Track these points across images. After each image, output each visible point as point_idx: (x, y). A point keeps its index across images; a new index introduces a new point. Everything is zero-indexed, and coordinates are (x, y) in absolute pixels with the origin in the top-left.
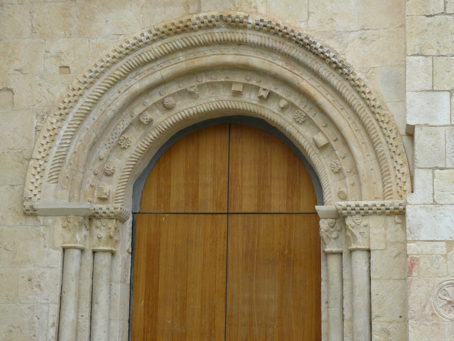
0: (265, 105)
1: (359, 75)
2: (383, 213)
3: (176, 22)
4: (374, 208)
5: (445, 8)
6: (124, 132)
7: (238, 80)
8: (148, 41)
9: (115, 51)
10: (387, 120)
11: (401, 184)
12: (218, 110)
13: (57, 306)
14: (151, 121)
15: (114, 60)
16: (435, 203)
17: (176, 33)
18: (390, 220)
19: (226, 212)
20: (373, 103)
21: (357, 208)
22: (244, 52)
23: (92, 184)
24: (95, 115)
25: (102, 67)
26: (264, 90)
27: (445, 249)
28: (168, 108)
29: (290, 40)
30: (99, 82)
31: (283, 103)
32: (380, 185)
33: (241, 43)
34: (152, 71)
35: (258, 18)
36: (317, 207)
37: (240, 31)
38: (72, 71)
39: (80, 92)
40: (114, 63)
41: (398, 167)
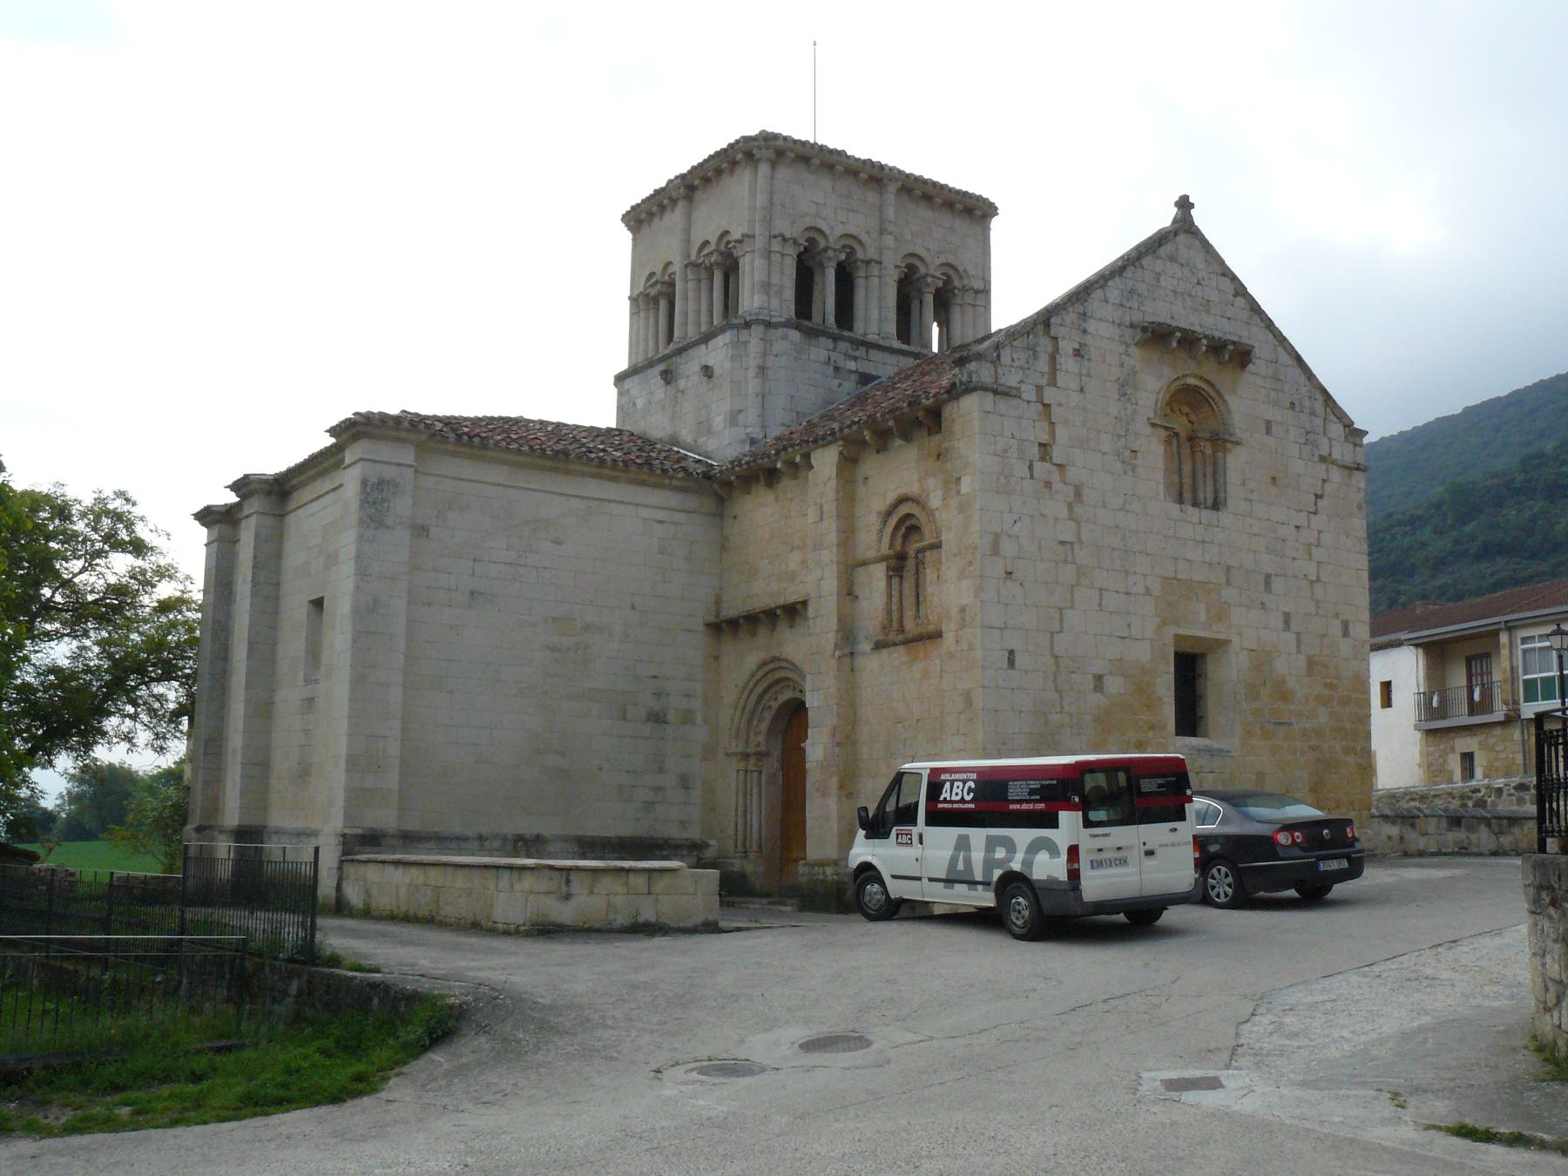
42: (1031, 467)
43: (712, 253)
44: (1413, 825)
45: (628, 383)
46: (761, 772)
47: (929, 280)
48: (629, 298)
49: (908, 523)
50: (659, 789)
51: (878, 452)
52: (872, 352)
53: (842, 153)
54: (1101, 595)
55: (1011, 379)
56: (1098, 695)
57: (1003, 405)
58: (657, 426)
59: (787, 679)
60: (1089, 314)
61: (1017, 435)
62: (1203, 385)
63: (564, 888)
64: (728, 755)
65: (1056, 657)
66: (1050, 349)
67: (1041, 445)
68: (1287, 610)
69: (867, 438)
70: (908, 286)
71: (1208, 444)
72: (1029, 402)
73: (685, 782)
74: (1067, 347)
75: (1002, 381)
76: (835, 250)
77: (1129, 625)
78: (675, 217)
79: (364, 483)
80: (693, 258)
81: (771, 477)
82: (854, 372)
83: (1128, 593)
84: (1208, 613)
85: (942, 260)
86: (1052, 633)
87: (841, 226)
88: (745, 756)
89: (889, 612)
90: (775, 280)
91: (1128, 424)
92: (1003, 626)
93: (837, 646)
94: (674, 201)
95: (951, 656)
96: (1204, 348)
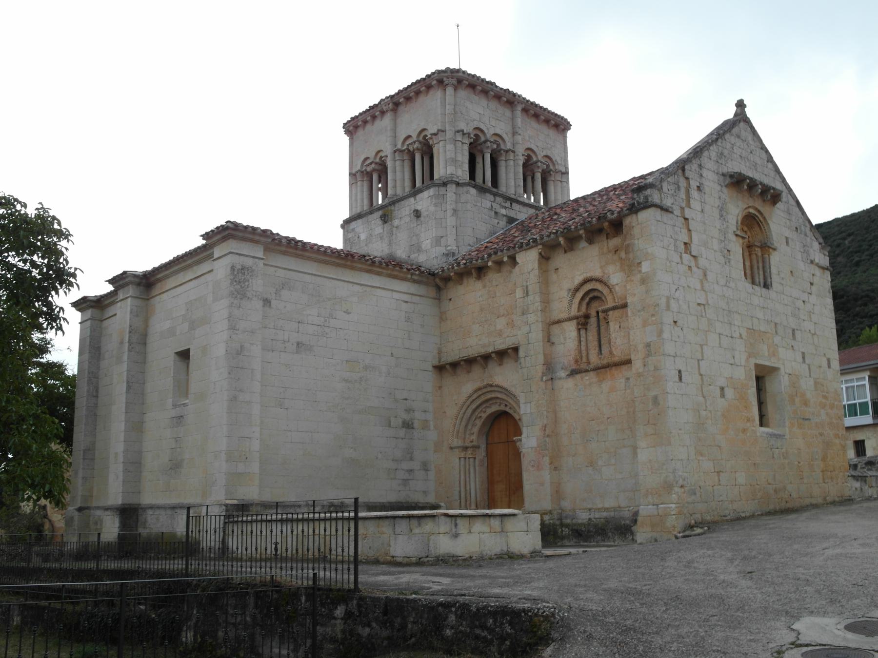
14: (481, 417)
24: (465, 417)
42: (681, 257)
43: (415, 142)
44: (865, 481)
45: (353, 225)
46: (475, 458)
47: (539, 164)
48: (350, 174)
49: (591, 295)
50: (411, 471)
51: (565, 252)
52: (514, 204)
53: (493, 84)
54: (720, 338)
55: (668, 202)
56: (723, 399)
57: (666, 217)
58: (378, 249)
59: (497, 398)
60: (703, 165)
61: (673, 236)
62: (757, 214)
63: (454, 530)
64: (451, 448)
65: (701, 375)
66: (685, 185)
67: (685, 244)
68: (803, 350)
69: (562, 242)
70: (528, 166)
71: (759, 249)
72: (677, 216)
73: (425, 467)
74: (694, 184)
75: (664, 202)
76: (491, 142)
77: (734, 357)
78: (387, 121)
79: (233, 268)
80: (399, 146)
81: (481, 271)
82: (505, 216)
83: (732, 337)
84: (768, 352)
85: (545, 153)
86: (698, 360)
87: (493, 128)
88: (465, 448)
89: (580, 352)
90: (459, 158)
91: (725, 234)
92: (675, 355)
93: (544, 374)
94: (383, 113)
95: (639, 375)
96: (760, 190)
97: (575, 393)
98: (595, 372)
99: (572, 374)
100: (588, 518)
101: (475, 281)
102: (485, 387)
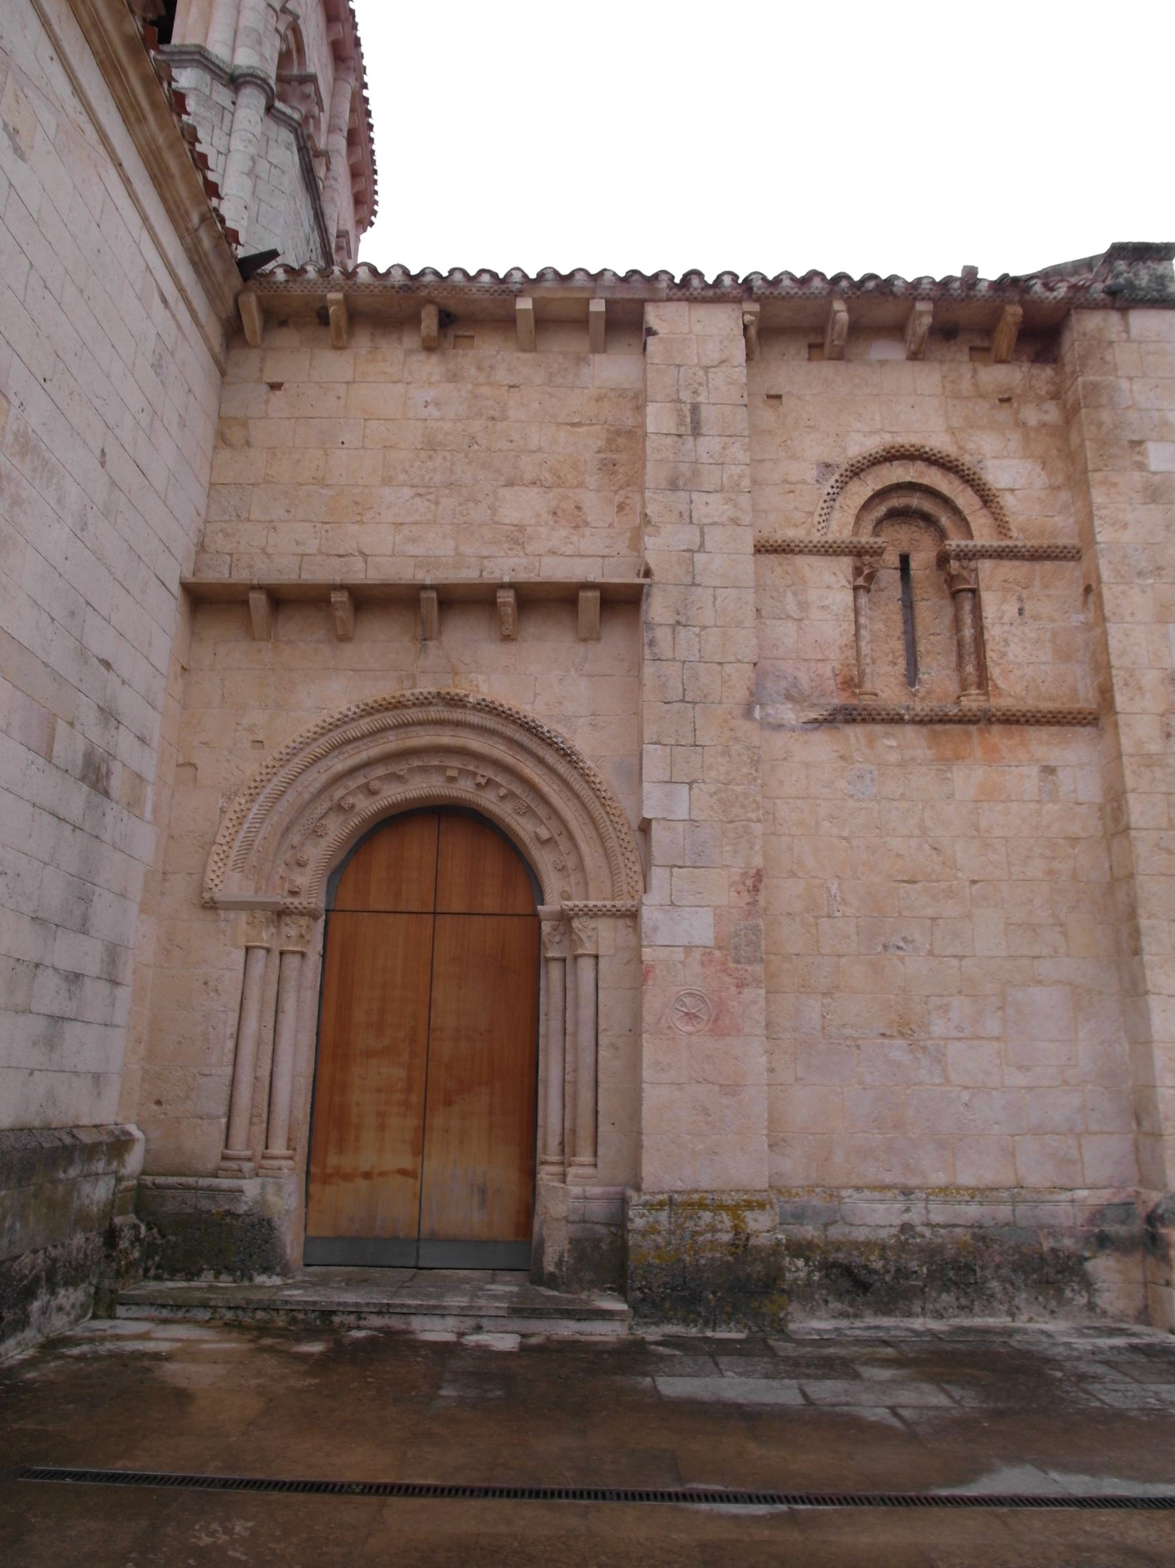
0: (482, 793)
1: (589, 763)
2: (613, 915)
3: (388, 697)
4: (604, 909)
5: (684, 695)
6: (321, 818)
7: (453, 764)
8: (354, 716)
9: (317, 726)
10: (618, 813)
11: (633, 884)
12: (428, 798)
13: (237, 1015)
14: (353, 806)
15: (316, 736)
16: (672, 904)
17: (387, 709)
18: (621, 923)
19: (432, 910)
20: (604, 794)
21: (585, 909)
22: (462, 734)
23: (284, 875)
24: (290, 796)
25: (301, 743)
26: (483, 776)
27: (682, 955)
28: (372, 793)
29: (514, 722)
30: (296, 760)
31: (502, 792)
32: (609, 884)
33: (458, 724)
34: (355, 751)
35: (480, 697)
36: (539, 907)
37: (459, 710)
38: (266, 746)
39: (274, 770)
40: (315, 739)
41: (630, 865)
49: (896, 502)
64: (211, 906)
97: (842, 784)
98: (924, 730)
99: (831, 722)
100: (898, 1222)
101: (409, 352)
102: (424, 702)
